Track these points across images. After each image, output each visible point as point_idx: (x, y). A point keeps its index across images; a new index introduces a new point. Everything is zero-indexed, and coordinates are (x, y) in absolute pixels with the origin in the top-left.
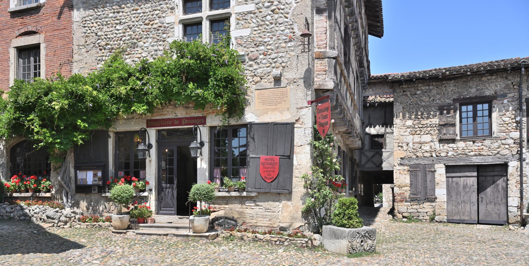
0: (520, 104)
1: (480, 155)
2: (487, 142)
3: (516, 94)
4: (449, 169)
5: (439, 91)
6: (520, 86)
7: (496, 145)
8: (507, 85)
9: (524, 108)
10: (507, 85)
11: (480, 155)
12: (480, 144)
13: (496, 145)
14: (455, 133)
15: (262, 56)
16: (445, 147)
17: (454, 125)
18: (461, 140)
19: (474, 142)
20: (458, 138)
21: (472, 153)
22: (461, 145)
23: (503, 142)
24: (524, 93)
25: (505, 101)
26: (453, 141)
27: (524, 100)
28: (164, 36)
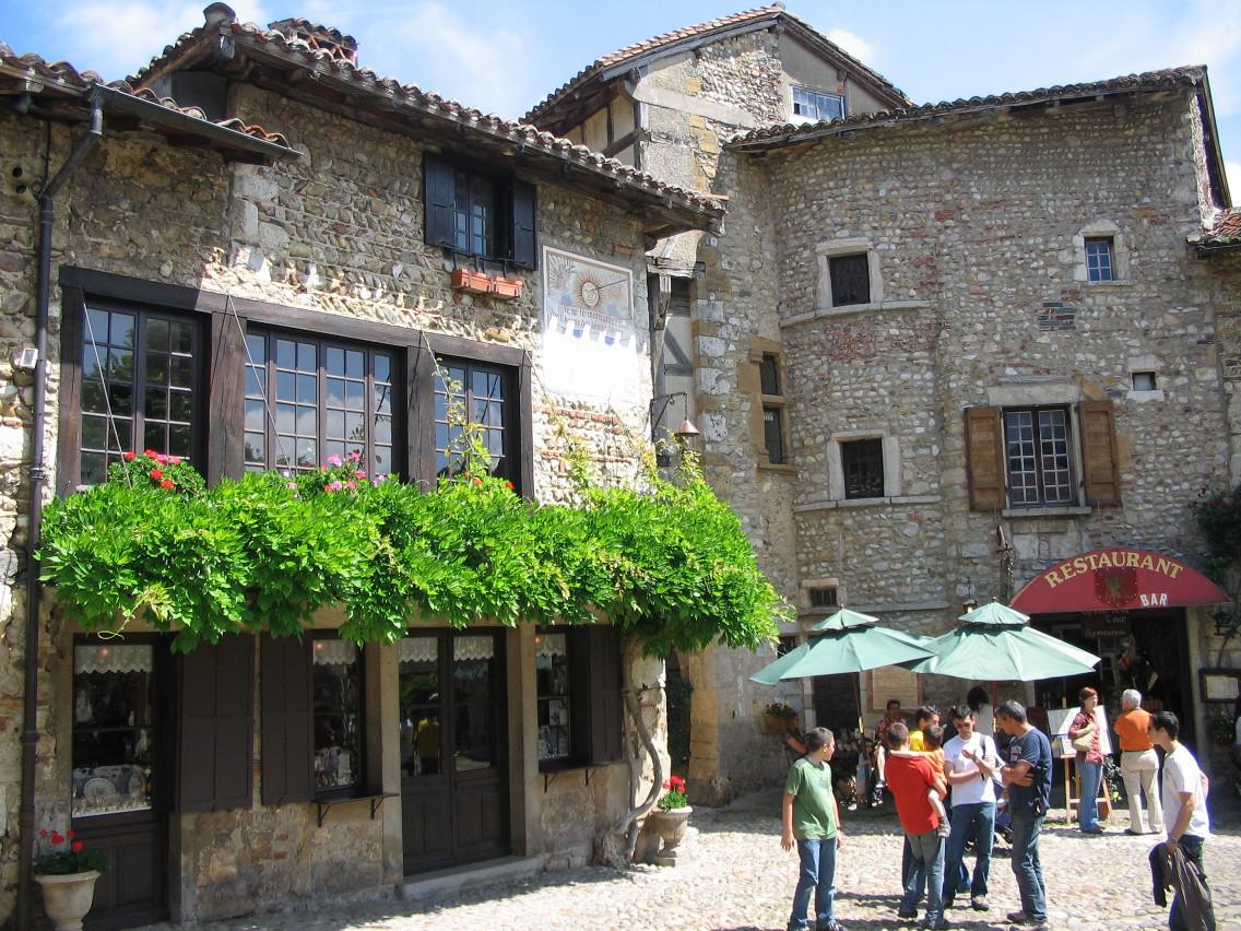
0: (39, 289)
3: (23, 233)
9: (55, 311)
24: (58, 240)
27: (54, 274)
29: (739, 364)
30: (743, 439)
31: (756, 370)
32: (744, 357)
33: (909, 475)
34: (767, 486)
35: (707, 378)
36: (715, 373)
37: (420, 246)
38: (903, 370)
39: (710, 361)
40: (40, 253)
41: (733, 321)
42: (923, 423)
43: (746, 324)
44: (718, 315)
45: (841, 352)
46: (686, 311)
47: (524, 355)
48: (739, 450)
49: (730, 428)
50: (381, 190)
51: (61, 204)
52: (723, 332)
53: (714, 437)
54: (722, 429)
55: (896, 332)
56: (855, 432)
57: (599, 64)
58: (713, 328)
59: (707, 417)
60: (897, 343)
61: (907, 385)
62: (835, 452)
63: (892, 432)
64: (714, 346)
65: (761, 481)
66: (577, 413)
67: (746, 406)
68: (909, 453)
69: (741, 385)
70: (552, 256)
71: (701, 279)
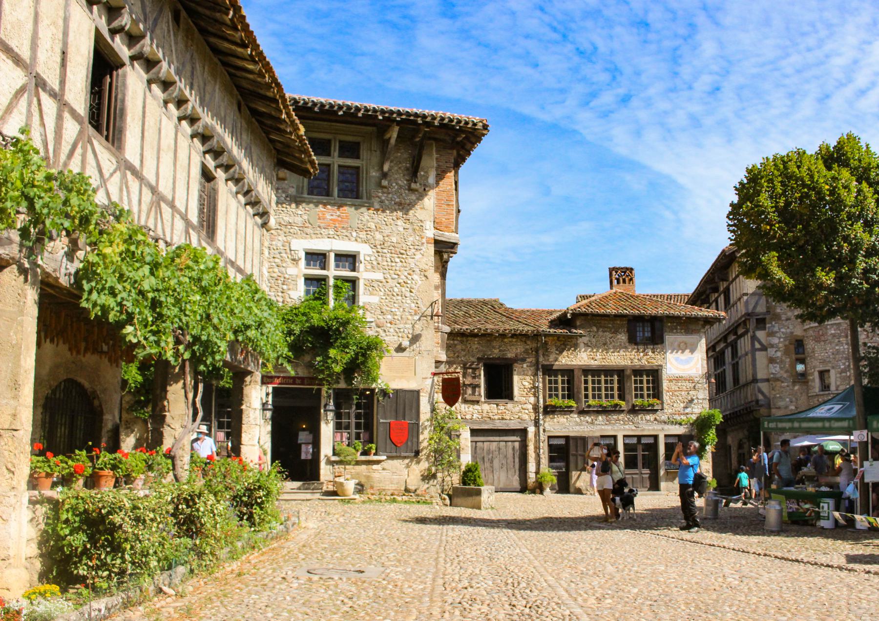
1: (503, 419)
2: (510, 405)
4: (474, 432)
5: (464, 347)
6: (537, 352)
7: (517, 409)
8: (526, 349)
10: (526, 349)
11: (503, 419)
12: (502, 408)
13: (517, 409)
14: (480, 395)
15: (389, 325)
16: (471, 409)
17: (478, 386)
18: (485, 402)
19: (497, 405)
20: (483, 399)
21: (496, 417)
22: (486, 407)
23: (524, 406)
24: (541, 359)
25: (525, 365)
26: (478, 402)
28: (285, 287)
29: (785, 346)
30: (787, 372)
31: (792, 347)
32: (787, 343)
33: (838, 383)
34: (796, 388)
35: (771, 352)
36: (775, 350)
37: (627, 344)
38: (837, 345)
39: (772, 346)
40: (537, 362)
41: (783, 330)
42: (844, 364)
43: (788, 331)
44: (776, 329)
45: (817, 340)
46: (764, 329)
47: (661, 366)
48: (785, 375)
49: (781, 368)
50: (616, 332)
51: (541, 352)
52: (778, 335)
53: (774, 372)
54: (778, 369)
55: (833, 332)
56: (822, 368)
57: (724, 251)
58: (771, 334)
59: (771, 365)
60: (834, 336)
61: (838, 352)
62: (816, 374)
63: (833, 368)
64: (775, 341)
65: (794, 386)
66: (678, 379)
67: (788, 360)
68: (838, 375)
69: (786, 352)
70: (669, 338)
71: (768, 317)
